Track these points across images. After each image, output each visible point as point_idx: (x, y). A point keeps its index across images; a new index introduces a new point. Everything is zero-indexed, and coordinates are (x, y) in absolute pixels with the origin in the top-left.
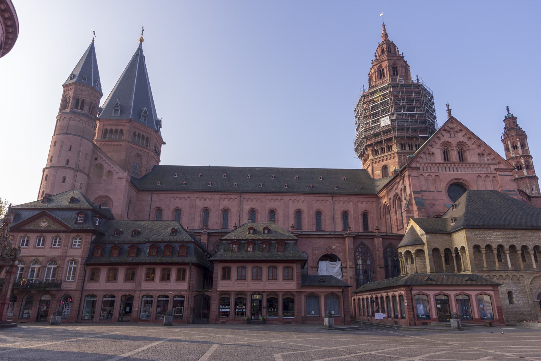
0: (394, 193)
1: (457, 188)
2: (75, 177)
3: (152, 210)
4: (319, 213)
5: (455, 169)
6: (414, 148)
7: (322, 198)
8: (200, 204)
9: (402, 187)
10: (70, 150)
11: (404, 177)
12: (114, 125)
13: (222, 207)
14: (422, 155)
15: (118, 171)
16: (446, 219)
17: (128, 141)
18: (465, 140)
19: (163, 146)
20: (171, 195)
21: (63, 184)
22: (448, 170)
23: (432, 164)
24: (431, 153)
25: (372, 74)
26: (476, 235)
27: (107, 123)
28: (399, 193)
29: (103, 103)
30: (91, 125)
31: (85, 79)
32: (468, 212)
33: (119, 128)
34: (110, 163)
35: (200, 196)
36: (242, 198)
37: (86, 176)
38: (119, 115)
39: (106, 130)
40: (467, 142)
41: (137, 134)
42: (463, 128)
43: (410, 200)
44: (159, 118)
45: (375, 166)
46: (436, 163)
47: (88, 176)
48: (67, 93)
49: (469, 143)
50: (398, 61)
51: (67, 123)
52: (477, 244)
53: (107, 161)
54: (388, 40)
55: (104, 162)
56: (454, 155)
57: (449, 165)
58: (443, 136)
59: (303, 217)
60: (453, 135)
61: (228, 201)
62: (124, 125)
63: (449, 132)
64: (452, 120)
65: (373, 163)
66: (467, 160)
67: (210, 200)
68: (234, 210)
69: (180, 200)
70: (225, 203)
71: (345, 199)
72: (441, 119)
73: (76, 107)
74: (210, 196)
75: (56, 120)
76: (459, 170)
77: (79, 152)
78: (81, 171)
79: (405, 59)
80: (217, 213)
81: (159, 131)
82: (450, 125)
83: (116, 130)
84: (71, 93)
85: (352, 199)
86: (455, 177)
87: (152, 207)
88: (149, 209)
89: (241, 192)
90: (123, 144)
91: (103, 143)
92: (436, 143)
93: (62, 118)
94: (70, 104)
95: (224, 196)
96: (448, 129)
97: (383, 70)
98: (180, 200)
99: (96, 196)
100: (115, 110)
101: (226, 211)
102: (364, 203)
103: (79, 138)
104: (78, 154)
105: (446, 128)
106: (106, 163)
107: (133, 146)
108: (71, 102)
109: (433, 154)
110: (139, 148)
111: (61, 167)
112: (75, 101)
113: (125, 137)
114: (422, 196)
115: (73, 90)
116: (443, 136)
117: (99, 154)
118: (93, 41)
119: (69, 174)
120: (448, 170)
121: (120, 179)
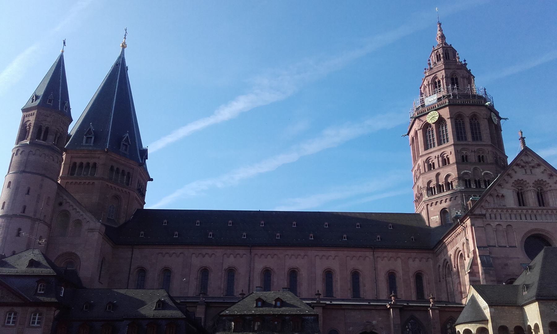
0: (455, 248)
1: (535, 242)
3: (132, 270)
4: (355, 275)
5: (533, 217)
6: (483, 186)
7: (359, 254)
9: (464, 240)
10: (28, 193)
11: (465, 228)
12: (86, 158)
14: (488, 198)
16: (518, 286)
17: (103, 179)
18: (545, 178)
19: (149, 182)
21: (17, 238)
22: (523, 217)
23: (502, 209)
24: (500, 195)
25: (425, 87)
28: (461, 249)
29: (72, 129)
30: (56, 160)
31: (50, 102)
32: (542, 278)
33: (92, 161)
34: (78, 210)
38: (92, 144)
39: (75, 164)
40: (548, 181)
41: (115, 168)
42: (542, 162)
43: (474, 259)
44: (144, 146)
45: (431, 209)
46: (507, 209)
47: (49, 226)
48: (26, 119)
49: (551, 182)
50: (458, 71)
51: (25, 158)
52: (553, 320)
53: (75, 207)
54: (446, 44)
55: (71, 208)
56: (531, 198)
57: (525, 211)
58: (516, 172)
59: (334, 280)
60: (529, 171)
61: (235, 257)
63: (523, 167)
64: (526, 151)
65: (428, 205)
66: (548, 204)
68: (242, 271)
70: (230, 261)
71: (391, 254)
72: (512, 151)
73: (38, 138)
74: (210, 251)
75: (12, 154)
76: (538, 217)
79: (468, 67)
81: (144, 163)
82: (523, 158)
83: (88, 164)
84: (32, 119)
85: (400, 254)
86: (534, 227)
90: (96, 182)
91: (70, 181)
92: (507, 183)
93: (20, 152)
94: (30, 134)
96: (523, 164)
97: (439, 82)
98: (170, 256)
100: (88, 138)
101: (231, 272)
102: (417, 260)
105: (519, 162)
107: (110, 184)
108: (31, 131)
109: (503, 196)
110: (117, 187)
113: (99, 173)
114: (490, 253)
115: (35, 115)
116: (516, 172)
117: (65, 197)
118: (63, 52)
120: (523, 217)
121: (91, 230)
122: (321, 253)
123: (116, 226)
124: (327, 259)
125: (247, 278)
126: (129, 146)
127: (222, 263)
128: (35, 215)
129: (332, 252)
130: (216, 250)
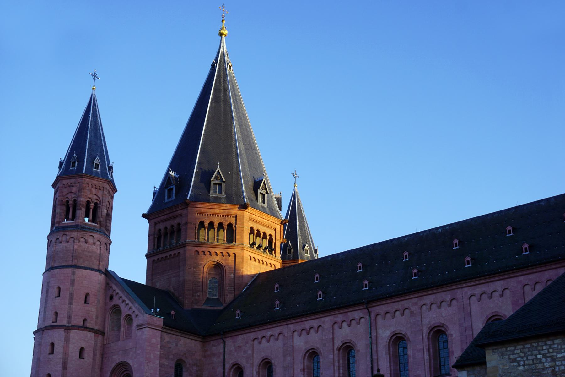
2: (67, 340)
3: (227, 371)
8: (301, 343)
13: (338, 344)
15: (137, 312)
20: (252, 336)
21: (51, 356)
26: (514, 360)
27: (159, 219)
30: (91, 240)
33: (175, 222)
34: (127, 301)
35: (299, 327)
36: (373, 315)
37: (90, 335)
38: (173, 198)
39: (160, 230)
47: (99, 332)
53: (124, 298)
61: (349, 325)
62: (181, 215)
67: (317, 332)
68: (361, 346)
69: (268, 341)
70: (344, 333)
74: (315, 323)
77: (71, 294)
78: (77, 327)
80: (331, 356)
87: (227, 366)
88: (222, 371)
89: (367, 302)
95: (340, 318)
98: (268, 341)
99: (113, 365)
103: (69, 270)
104: (71, 299)
106: (124, 301)
111: (48, 328)
112: (64, 208)
117: (114, 287)
119: (58, 336)
121: (140, 327)
122: (478, 291)
123: (220, 308)
124: (490, 298)
125: (369, 357)
126: (223, 184)
127: (333, 339)
128: (69, 322)
129: (498, 283)
130: (323, 319)
